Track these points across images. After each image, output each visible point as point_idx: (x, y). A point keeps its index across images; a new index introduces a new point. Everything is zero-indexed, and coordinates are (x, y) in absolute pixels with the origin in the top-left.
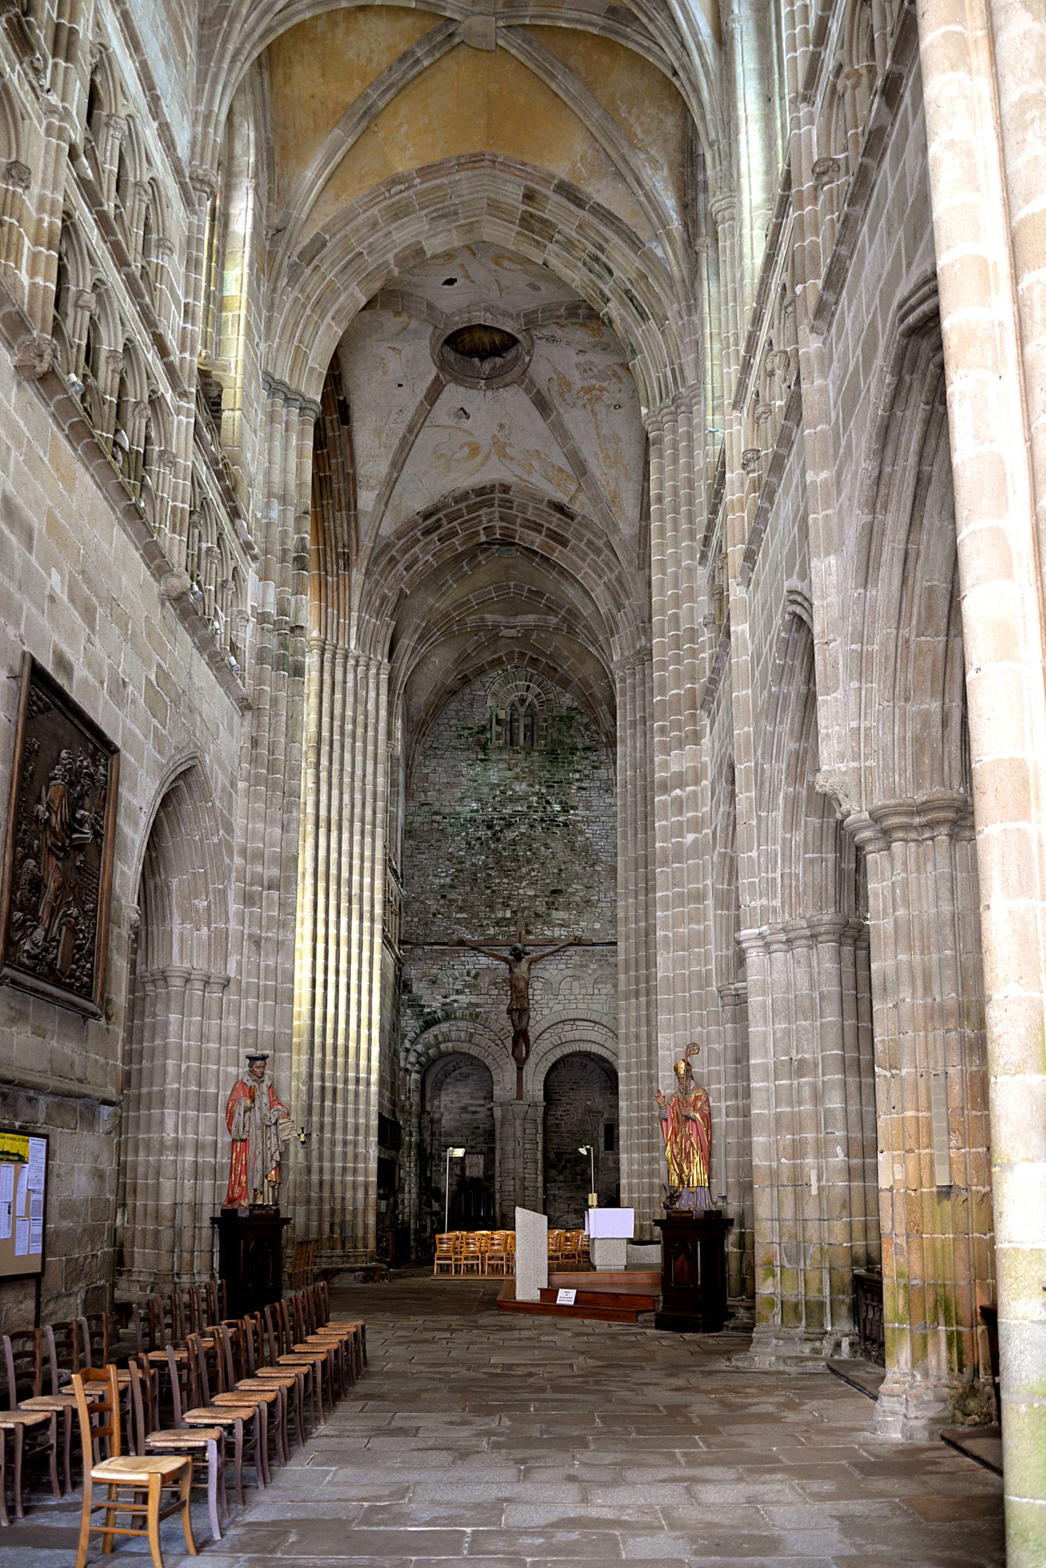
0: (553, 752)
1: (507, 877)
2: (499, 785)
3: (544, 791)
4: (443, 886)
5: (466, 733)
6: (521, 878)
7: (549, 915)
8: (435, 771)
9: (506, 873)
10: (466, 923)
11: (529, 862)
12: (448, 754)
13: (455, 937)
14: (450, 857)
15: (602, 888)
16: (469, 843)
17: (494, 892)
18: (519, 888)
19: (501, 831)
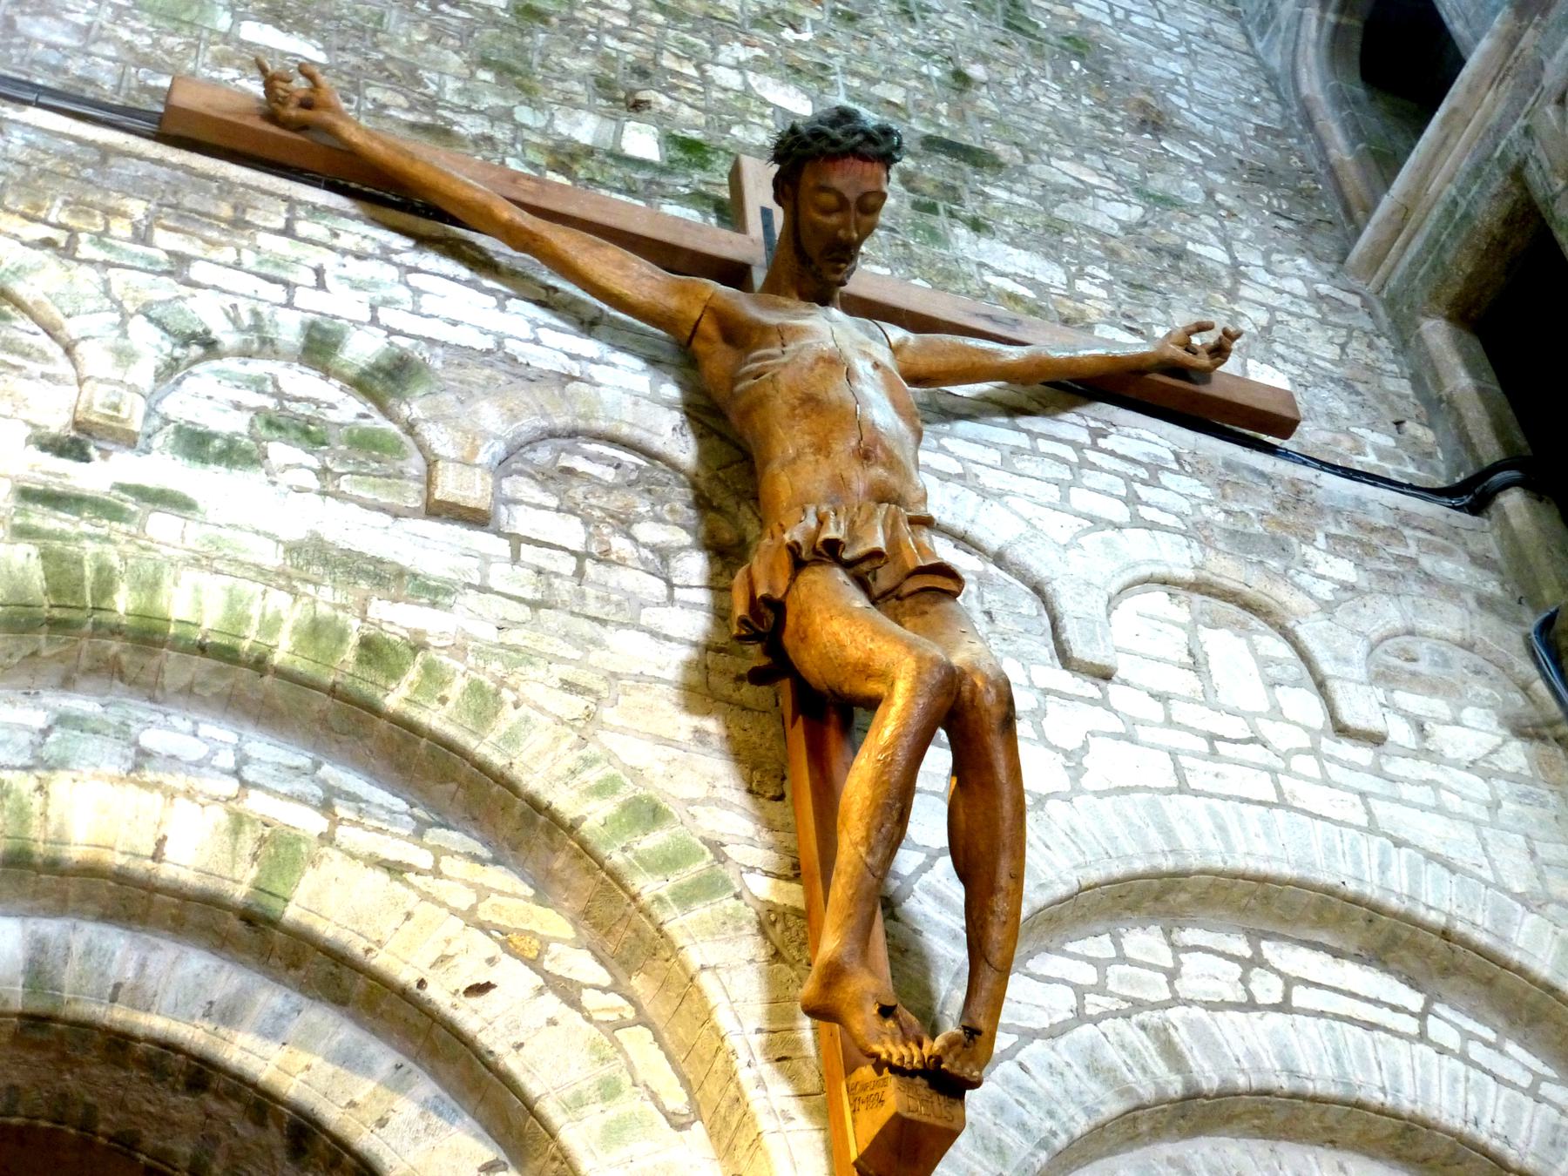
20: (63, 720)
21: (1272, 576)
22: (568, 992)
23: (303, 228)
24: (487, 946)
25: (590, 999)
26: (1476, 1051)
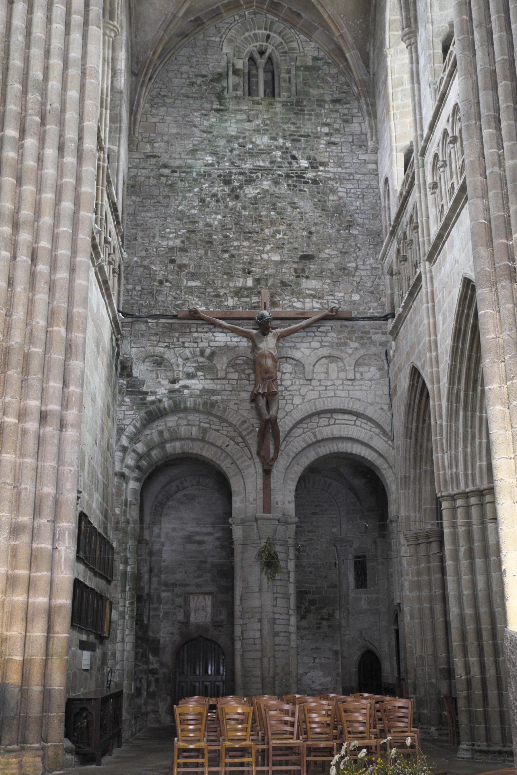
0: (299, 103)
1: (247, 239)
2: (237, 138)
3: (289, 145)
4: (171, 249)
5: (199, 81)
6: (265, 241)
7: (298, 284)
8: (163, 119)
9: (248, 235)
10: (201, 293)
11: (273, 223)
12: (178, 102)
13: (185, 309)
14: (181, 217)
15: (360, 253)
16: (202, 201)
17: (232, 256)
18: (262, 252)
19: (241, 187)
20: (179, 418)
21: (342, 351)
22: (238, 444)
23: (199, 330)
24: (228, 439)
25: (240, 444)
26: (363, 425)
